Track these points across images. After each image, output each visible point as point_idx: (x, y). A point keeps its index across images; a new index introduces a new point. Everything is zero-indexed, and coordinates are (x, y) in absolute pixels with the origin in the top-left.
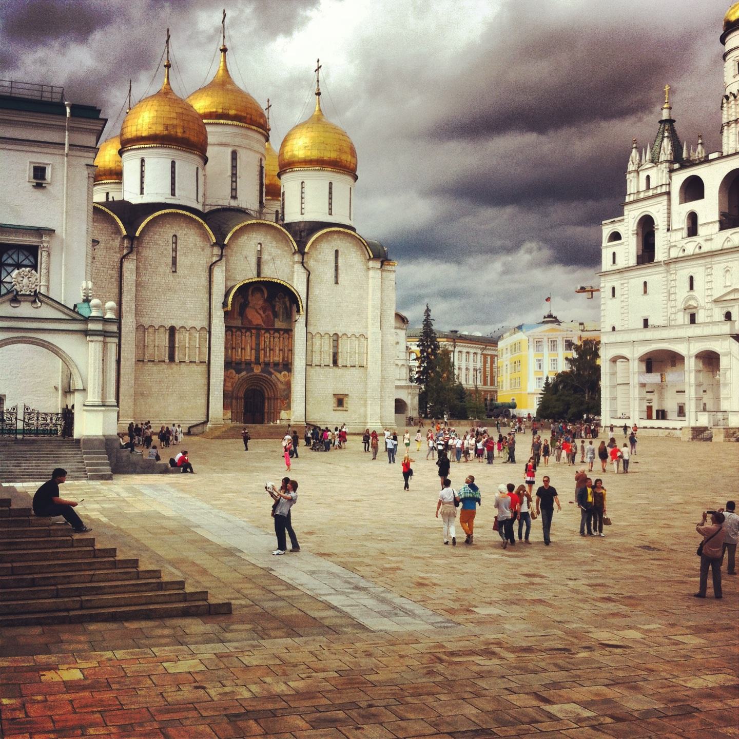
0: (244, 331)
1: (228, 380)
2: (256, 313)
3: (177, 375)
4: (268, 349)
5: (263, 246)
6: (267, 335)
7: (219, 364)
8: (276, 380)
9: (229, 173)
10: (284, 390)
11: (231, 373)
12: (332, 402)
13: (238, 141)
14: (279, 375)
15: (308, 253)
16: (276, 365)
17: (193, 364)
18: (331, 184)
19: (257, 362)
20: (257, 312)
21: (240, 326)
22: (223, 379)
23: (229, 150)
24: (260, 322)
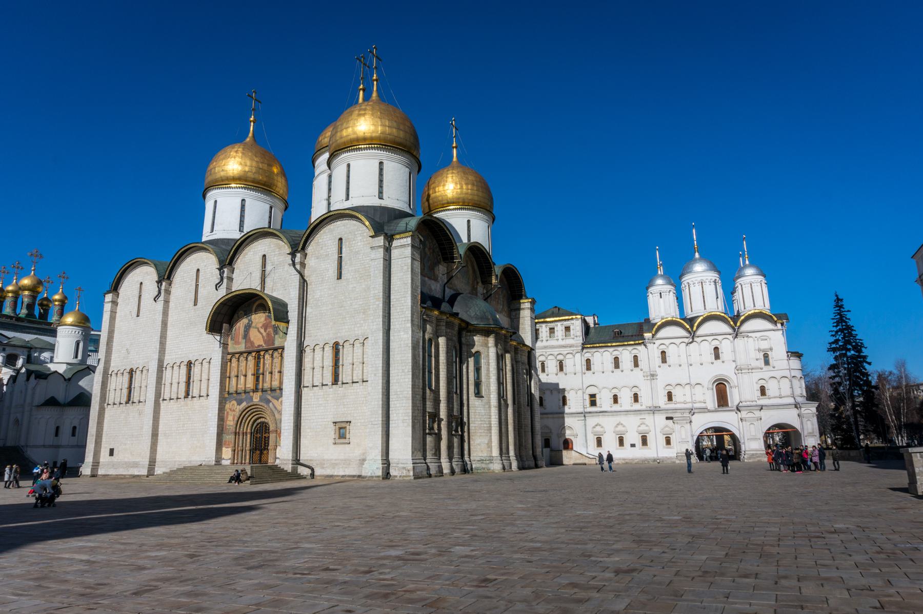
1: (230, 413)
2: (258, 333)
3: (190, 412)
4: (267, 373)
7: (215, 396)
9: (326, 196)
11: (233, 405)
12: (331, 432)
14: (274, 401)
16: (272, 390)
18: (349, 165)
19: (256, 390)
20: (259, 331)
21: (243, 350)
22: (217, 412)
24: (262, 343)
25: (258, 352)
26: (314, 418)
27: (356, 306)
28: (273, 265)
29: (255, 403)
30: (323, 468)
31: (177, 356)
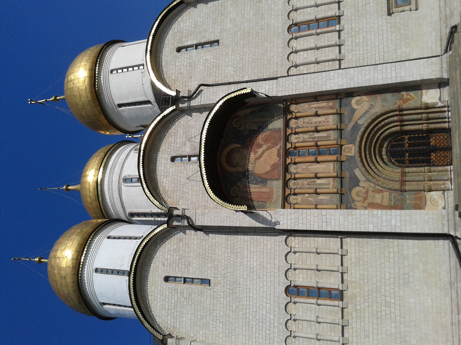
0: (288, 176)
1: (370, 200)
2: (262, 159)
3: (366, 288)
4: (316, 135)
5: (174, 154)
6: (293, 138)
8: (368, 115)
10: (384, 100)
13: (115, 178)
14: (357, 115)
15: (178, 92)
17: (344, 260)
18: (112, 71)
22: (366, 211)
23: (124, 188)
24: (275, 151)
25: (287, 153)
26: (381, 46)
27: (252, 14)
28: (185, 144)
29: (357, 149)
30: (452, 14)
31: (276, 324)
